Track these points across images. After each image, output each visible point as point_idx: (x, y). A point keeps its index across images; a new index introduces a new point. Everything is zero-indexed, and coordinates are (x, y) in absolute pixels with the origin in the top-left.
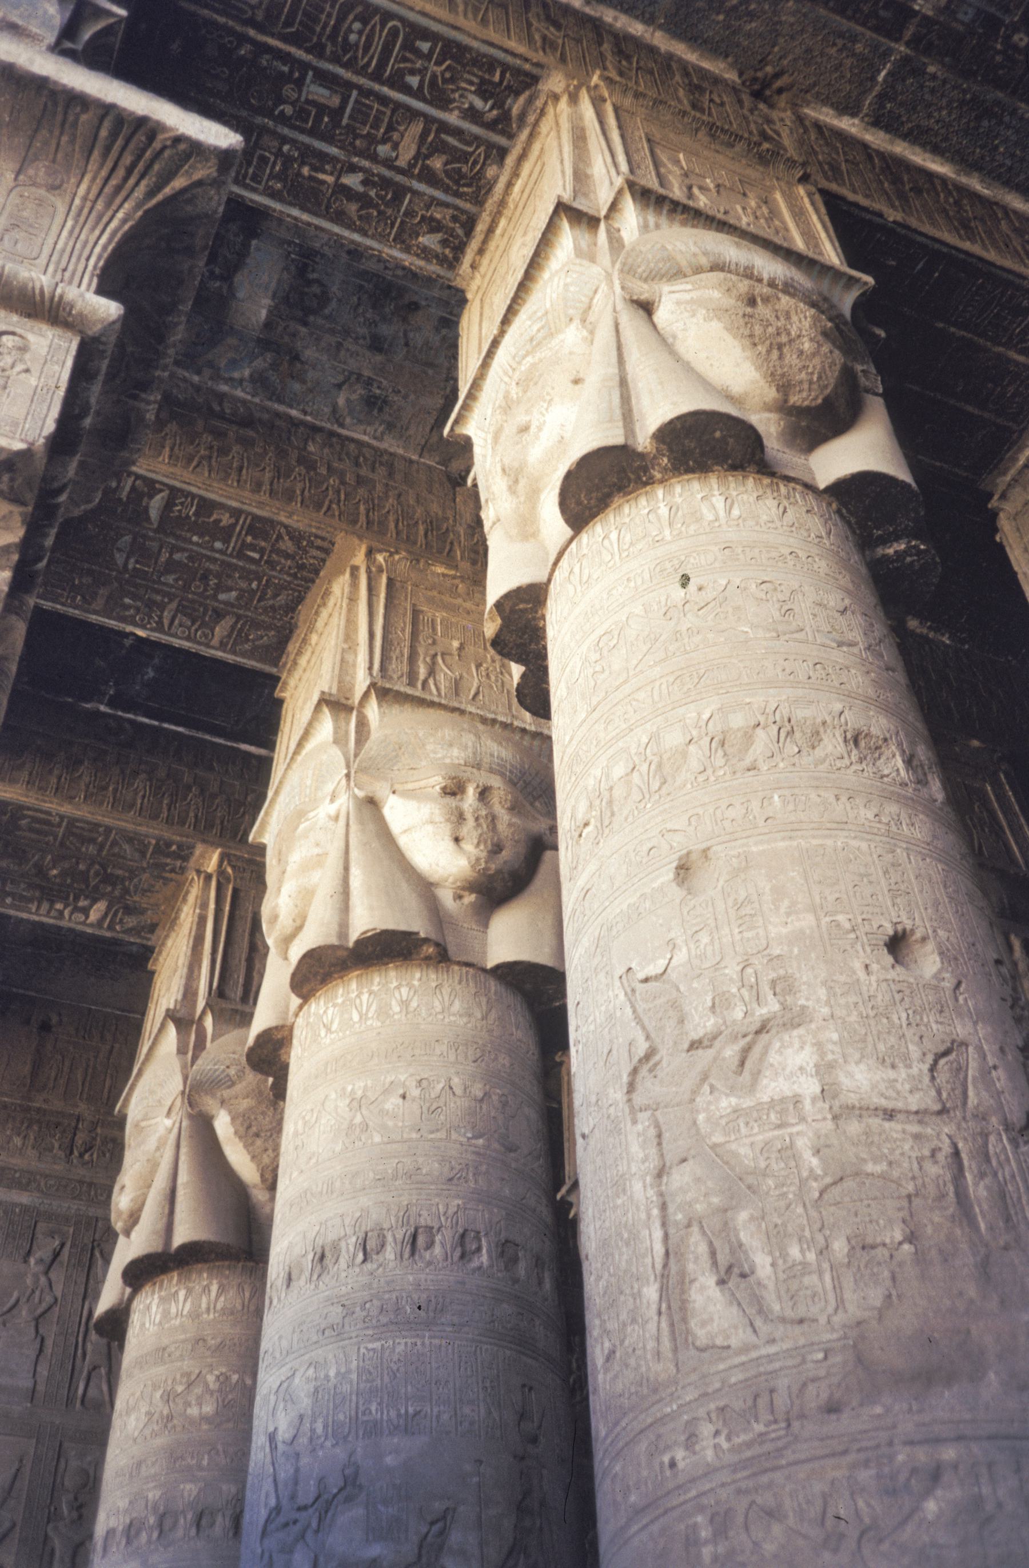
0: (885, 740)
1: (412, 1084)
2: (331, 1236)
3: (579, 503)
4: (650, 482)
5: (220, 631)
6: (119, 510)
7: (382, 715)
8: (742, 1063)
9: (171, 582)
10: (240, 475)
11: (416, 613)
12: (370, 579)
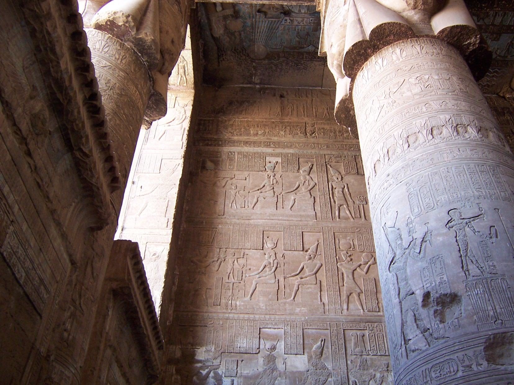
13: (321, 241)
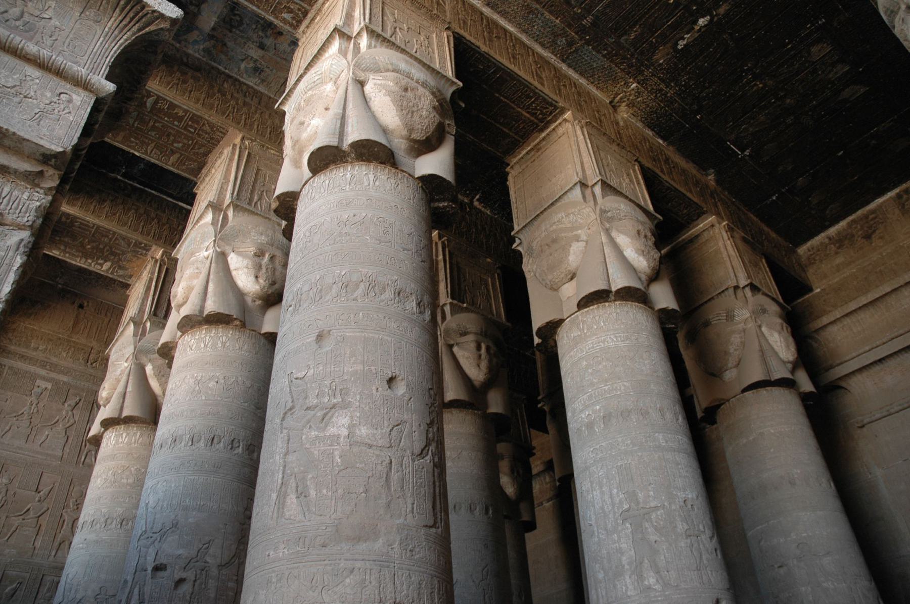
0: (411, 294)
1: (221, 378)
2: (180, 433)
3: (316, 164)
4: (346, 162)
5: (173, 159)
7: (234, 216)
8: (323, 419)
10: (190, 94)
11: (258, 170)
12: (240, 152)
13: (57, 485)
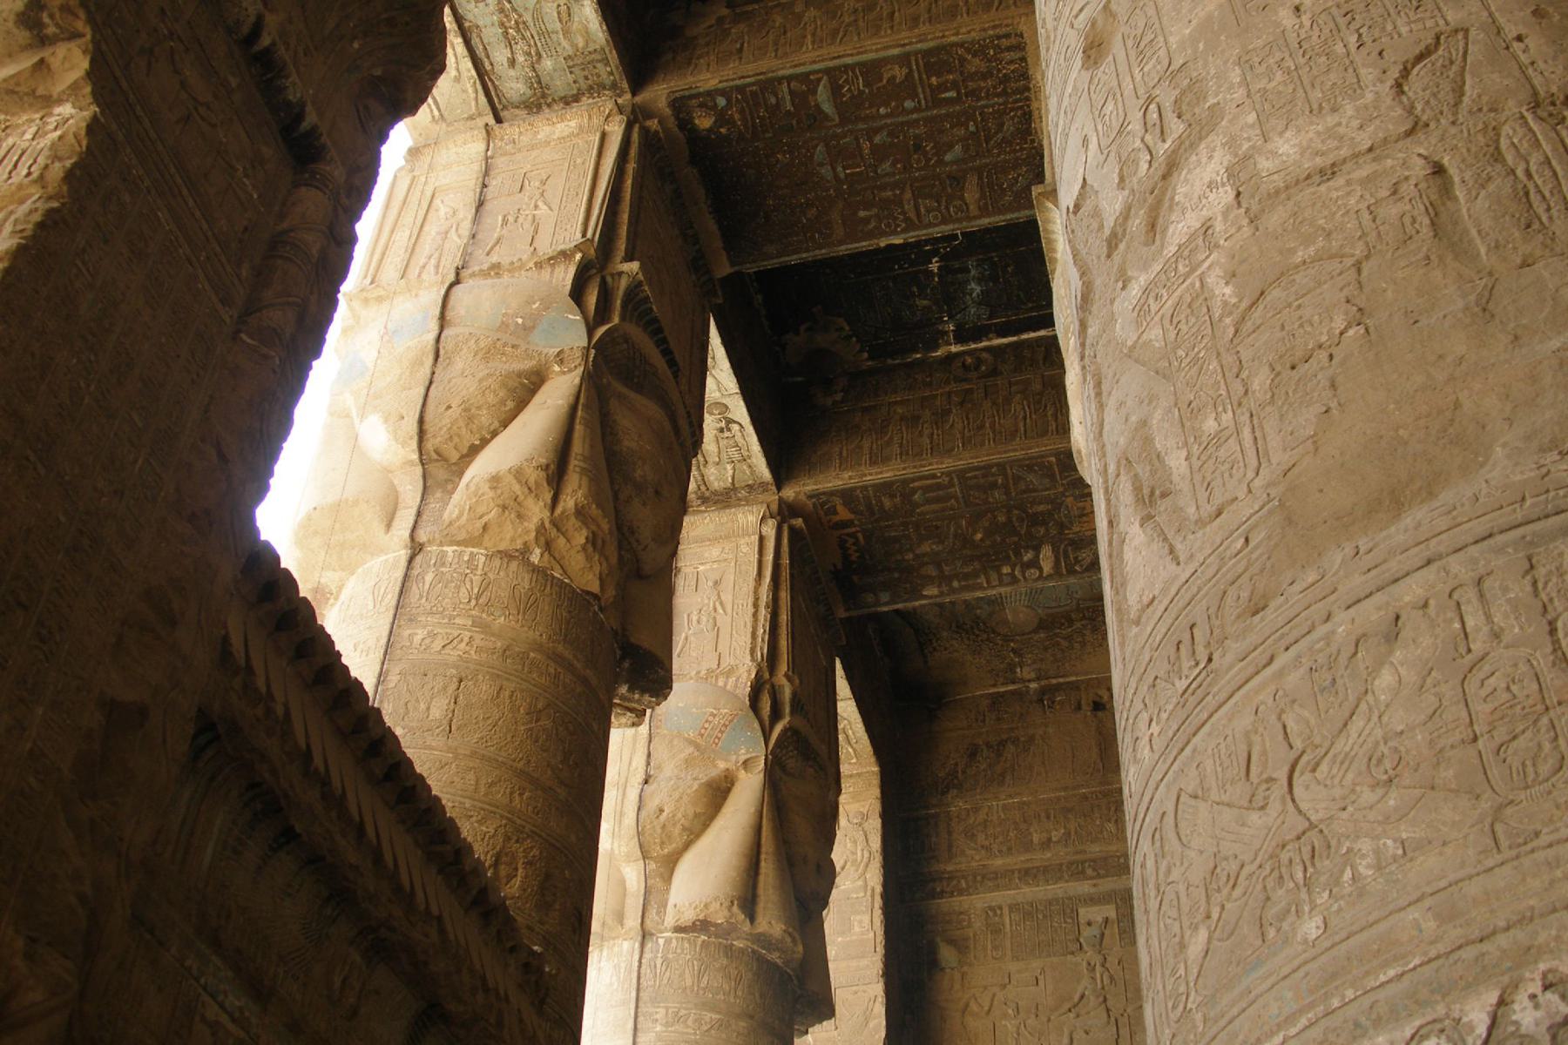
5: (971, 195)
6: (794, 122)
9: (889, 170)
